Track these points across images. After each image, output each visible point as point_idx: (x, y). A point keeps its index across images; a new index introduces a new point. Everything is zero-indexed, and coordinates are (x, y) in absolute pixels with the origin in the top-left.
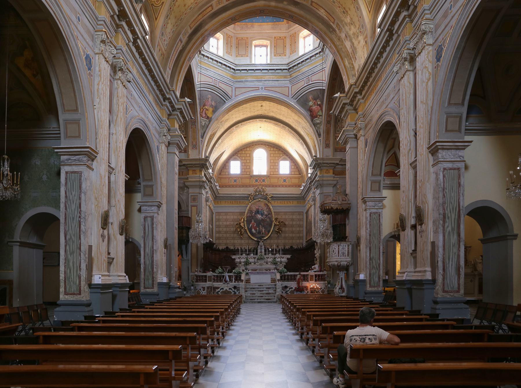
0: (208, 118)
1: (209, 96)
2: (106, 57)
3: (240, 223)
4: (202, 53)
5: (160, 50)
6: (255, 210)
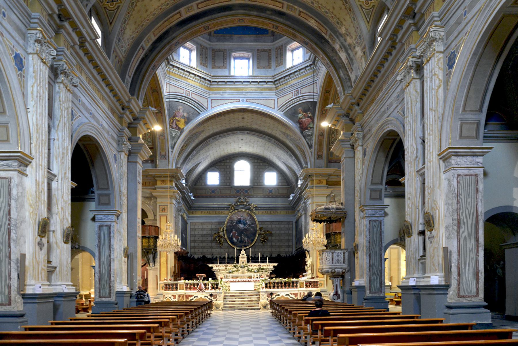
0: (179, 129)
1: (180, 107)
2: (43, 57)
3: (219, 233)
4: (171, 63)
5: (116, 57)
6: (237, 220)
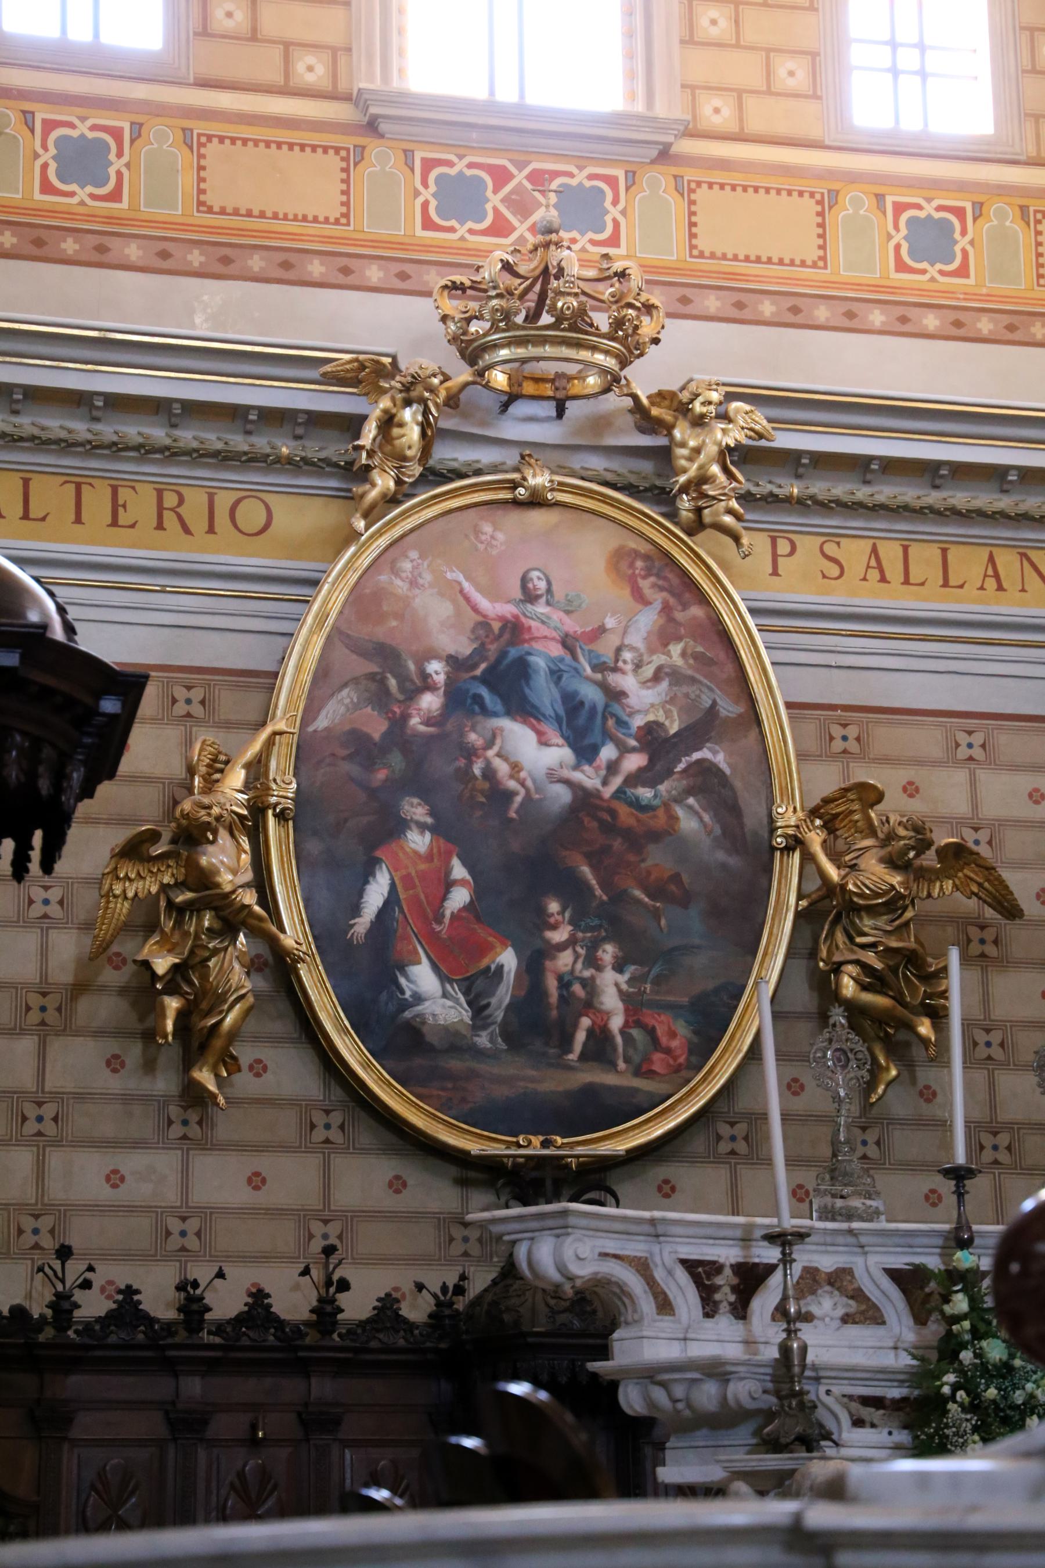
6: (464, 648)
